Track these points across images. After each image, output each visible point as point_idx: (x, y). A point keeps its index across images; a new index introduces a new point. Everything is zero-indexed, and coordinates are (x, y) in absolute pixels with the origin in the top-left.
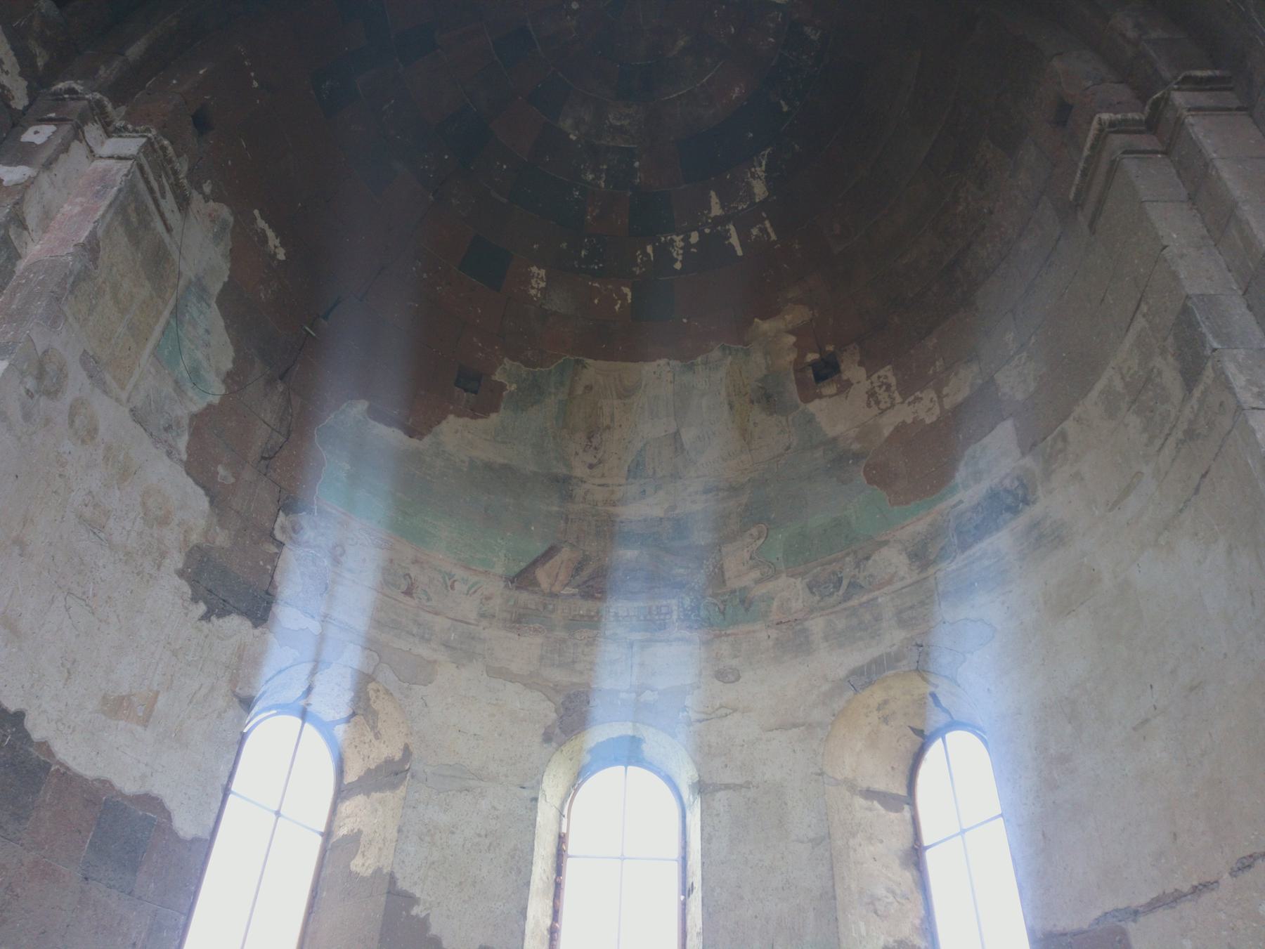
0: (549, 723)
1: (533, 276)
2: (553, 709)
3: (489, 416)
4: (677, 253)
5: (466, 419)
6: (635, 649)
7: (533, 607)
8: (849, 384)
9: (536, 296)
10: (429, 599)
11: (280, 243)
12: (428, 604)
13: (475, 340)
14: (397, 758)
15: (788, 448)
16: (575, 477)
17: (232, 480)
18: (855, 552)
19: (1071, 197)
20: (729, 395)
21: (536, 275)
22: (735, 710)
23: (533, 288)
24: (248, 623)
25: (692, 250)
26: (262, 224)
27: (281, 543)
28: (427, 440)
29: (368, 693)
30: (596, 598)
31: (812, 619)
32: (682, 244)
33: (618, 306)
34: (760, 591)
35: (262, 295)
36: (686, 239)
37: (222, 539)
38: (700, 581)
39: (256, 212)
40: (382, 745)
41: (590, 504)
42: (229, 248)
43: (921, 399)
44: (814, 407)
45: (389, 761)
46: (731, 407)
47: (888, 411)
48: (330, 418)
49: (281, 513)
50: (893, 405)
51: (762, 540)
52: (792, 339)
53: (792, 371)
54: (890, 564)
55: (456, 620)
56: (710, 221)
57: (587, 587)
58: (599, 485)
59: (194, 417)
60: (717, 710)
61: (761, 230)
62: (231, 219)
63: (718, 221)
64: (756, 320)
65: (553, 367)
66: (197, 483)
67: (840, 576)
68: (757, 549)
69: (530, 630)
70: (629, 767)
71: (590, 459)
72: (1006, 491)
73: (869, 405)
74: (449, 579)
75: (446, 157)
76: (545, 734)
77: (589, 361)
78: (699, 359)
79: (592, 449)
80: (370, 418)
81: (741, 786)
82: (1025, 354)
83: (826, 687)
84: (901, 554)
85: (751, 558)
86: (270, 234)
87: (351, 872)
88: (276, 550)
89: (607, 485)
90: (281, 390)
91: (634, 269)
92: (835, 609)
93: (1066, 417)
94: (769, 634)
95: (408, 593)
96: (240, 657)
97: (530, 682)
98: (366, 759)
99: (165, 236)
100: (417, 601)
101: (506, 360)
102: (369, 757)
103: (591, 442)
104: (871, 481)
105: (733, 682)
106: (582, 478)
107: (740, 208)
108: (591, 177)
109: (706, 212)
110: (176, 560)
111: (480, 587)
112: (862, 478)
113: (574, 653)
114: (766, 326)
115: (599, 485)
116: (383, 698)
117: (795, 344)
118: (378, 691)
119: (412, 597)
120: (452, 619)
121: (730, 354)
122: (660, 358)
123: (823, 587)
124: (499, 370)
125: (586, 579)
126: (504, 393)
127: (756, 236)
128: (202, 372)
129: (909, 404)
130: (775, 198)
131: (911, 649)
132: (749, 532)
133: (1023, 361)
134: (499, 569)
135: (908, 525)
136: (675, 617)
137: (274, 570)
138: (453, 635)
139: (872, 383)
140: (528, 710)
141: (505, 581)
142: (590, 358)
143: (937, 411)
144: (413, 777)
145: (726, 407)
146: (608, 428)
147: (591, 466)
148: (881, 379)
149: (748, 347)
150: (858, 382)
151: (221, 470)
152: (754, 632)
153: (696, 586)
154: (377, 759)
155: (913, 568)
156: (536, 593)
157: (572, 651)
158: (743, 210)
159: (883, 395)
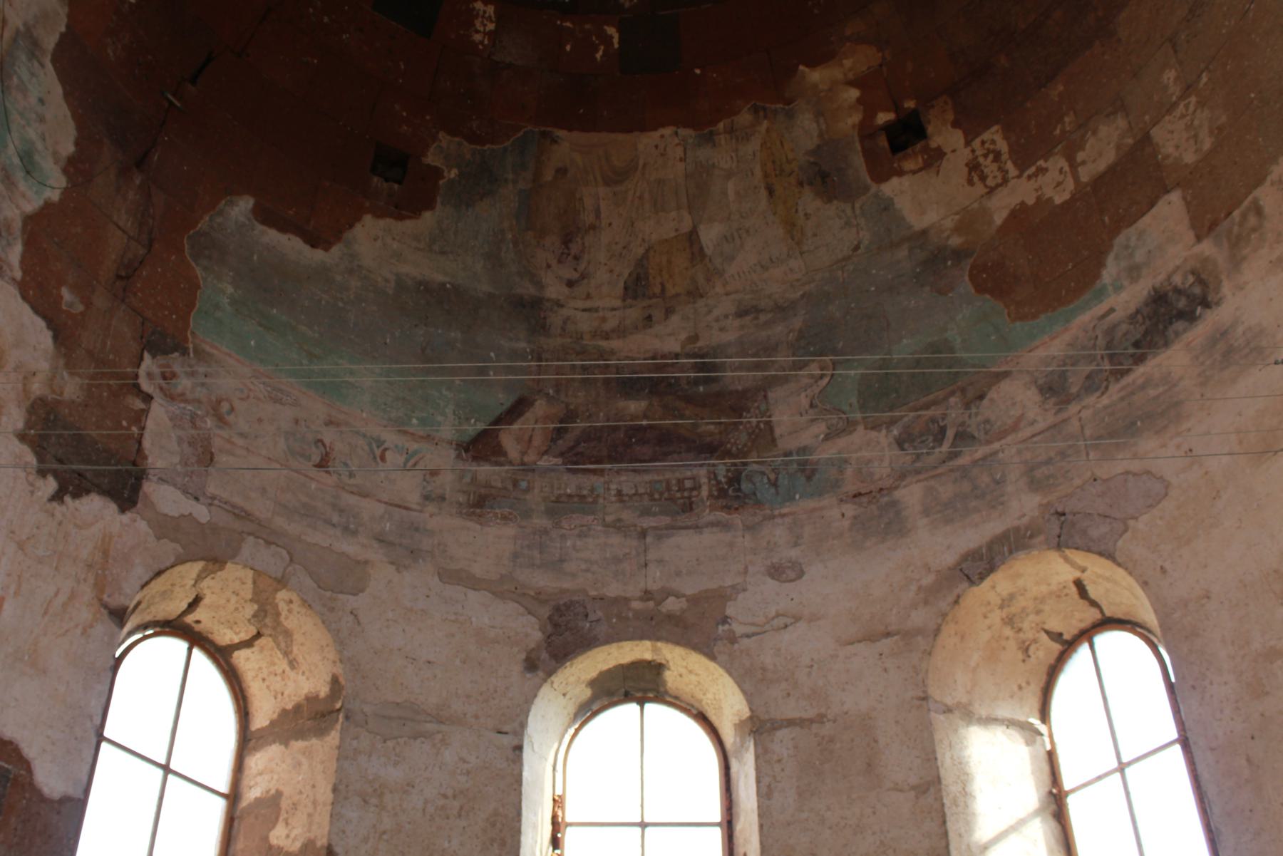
0: (532, 645)
1: (478, 14)
2: (537, 627)
3: (420, 214)
6: (649, 540)
7: (499, 485)
9: (482, 42)
10: (351, 475)
12: (352, 481)
13: (397, 107)
14: (322, 695)
15: (857, 248)
16: (548, 300)
17: (81, 308)
18: (963, 391)
20: (766, 176)
21: (481, 13)
22: (797, 619)
23: (477, 32)
24: (113, 507)
28: (336, 250)
29: (277, 606)
31: (905, 486)
34: (828, 452)
35: (110, 52)
37: (72, 388)
38: (738, 442)
41: (571, 337)
44: (891, 187)
45: (311, 699)
46: (771, 191)
48: (202, 221)
52: (854, 93)
53: (857, 139)
55: (391, 505)
58: (584, 310)
59: (29, 220)
60: (773, 619)
64: (801, 68)
65: (508, 144)
66: (36, 311)
67: (942, 424)
68: (821, 392)
69: (497, 517)
70: (648, 706)
71: (568, 273)
74: (378, 447)
77: (561, 133)
78: (721, 125)
79: (570, 258)
80: (257, 220)
81: (811, 721)
85: (812, 406)
87: (271, 847)
88: (142, 406)
92: (940, 471)
94: (844, 511)
95: (322, 464)
96: (106, 553)
97: (503, 589)
98: (279, 696)
100: (335, 477)
101: (441, 135)
102: (282, 694)
103: (568, 248)
106: (559, 300)
110: (16, 418)
111: (421, 459)
112: (966, 286)
113: (561, 548)
114: (816, 76)
115: (584, 310)
117: (859, 100)
118: (291, 602)
119: (328, 472)
120: (386, 503)
121: (765, 117)
123: (919, 441)
124: (432, 150)
125: (572, 444)
126: (441, 182)
128: (37, 158)
134: (447, 430)
136: (705, 492)
138: (388, 525)
140: (501, 628)
141: (456, 450)
142: (562, 128)
144: (347, 718)
145: (763, 193)
146: (593, 227)
147: (570, 284)
149: (791, 106)
151: (66, 294)
152: (822, 509)
153: (734, 449)
154: (295, 695)
157: (558, 545)
159: (990, 167)
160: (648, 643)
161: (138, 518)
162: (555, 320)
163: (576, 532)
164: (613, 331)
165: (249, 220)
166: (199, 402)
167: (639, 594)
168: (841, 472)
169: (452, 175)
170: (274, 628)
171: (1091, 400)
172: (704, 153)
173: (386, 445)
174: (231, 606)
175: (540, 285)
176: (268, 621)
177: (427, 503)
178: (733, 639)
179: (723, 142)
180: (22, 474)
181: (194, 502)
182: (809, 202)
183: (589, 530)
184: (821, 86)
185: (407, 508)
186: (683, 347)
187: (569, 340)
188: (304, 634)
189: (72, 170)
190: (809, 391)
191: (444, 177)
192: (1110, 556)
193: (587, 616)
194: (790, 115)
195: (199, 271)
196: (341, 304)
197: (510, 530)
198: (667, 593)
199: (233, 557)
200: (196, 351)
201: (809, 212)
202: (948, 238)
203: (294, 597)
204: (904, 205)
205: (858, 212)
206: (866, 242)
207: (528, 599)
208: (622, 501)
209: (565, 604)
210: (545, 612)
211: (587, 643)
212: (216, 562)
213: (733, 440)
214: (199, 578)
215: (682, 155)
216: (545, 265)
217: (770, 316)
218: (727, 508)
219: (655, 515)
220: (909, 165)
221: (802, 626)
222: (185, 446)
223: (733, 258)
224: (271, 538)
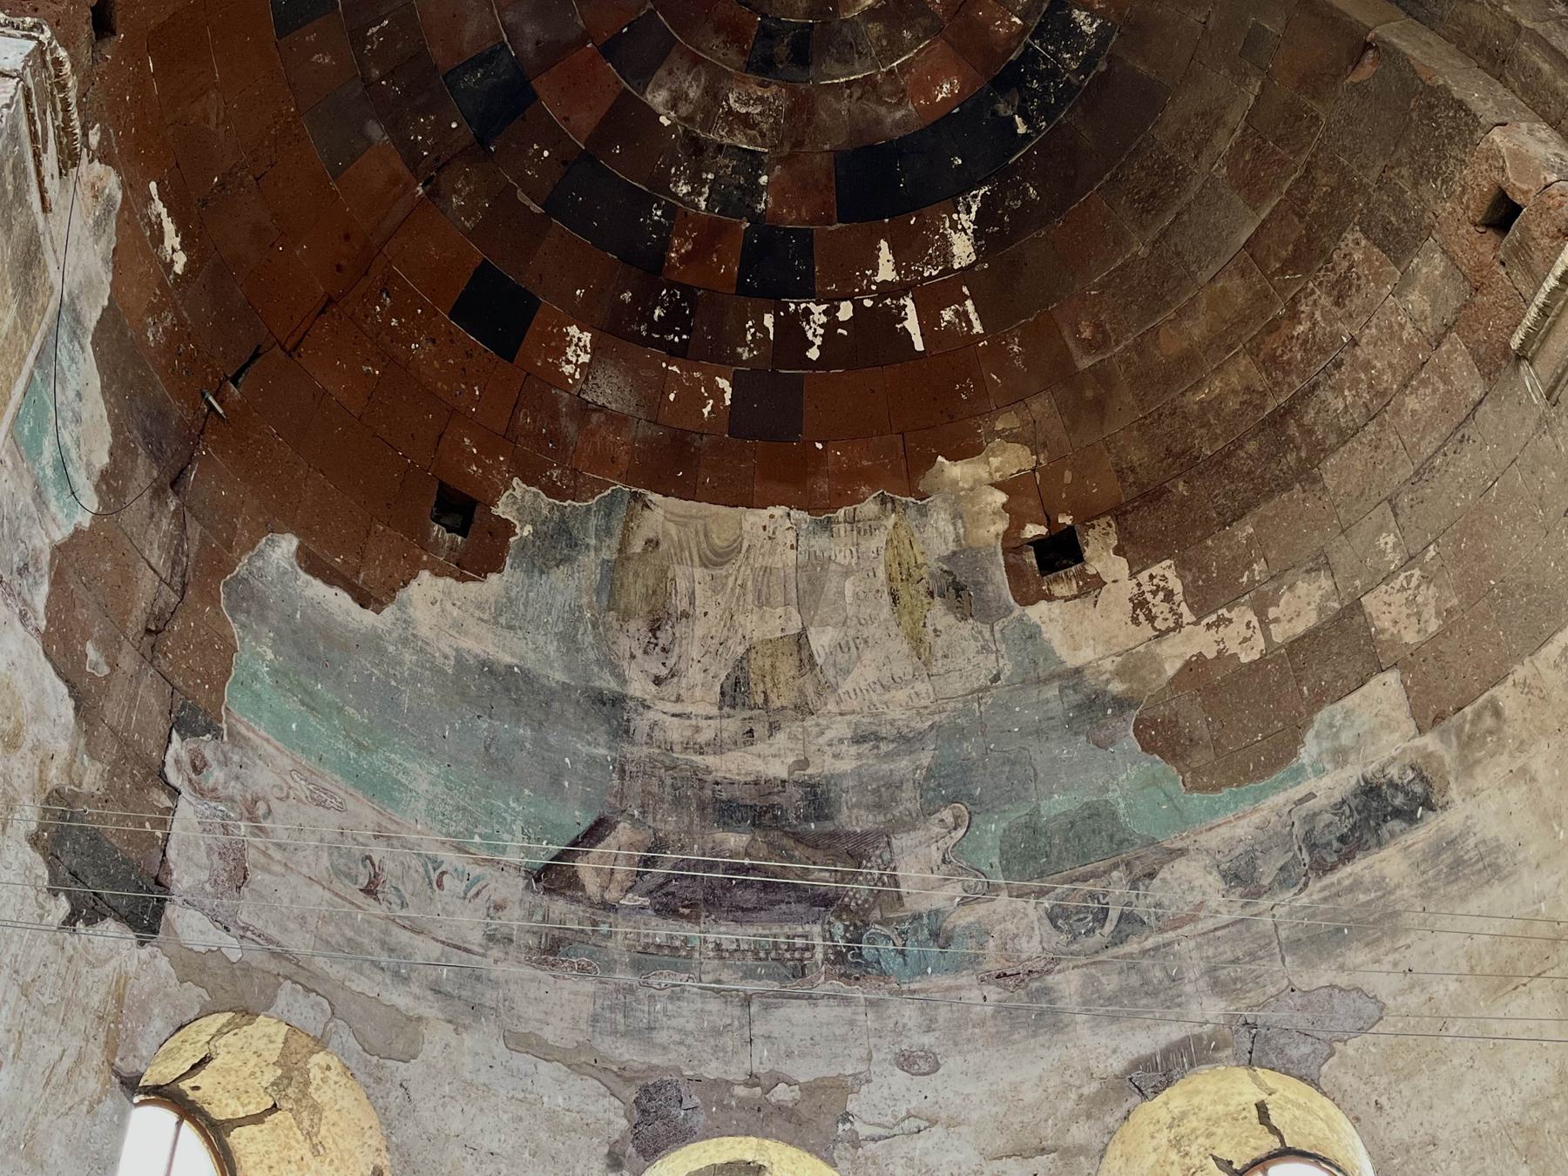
2: (622, 1112)
3: (485, 577)
4: (814, 332)
5: (449, 581)
6: (753, 1009)
8: (1098, 582)
9: (572, 376)
10: (403, 905)
11: (181, 244)
15: (996, 678)
17: (106, 670)
19: (1515, 343)
20: (890, 579)
21: (575, 340)
22: (933, 1122)
23: (569, 362)
25: (840, 331)
26: (159, 207)
27: (176, 790)
28: (389, 612)
30: (682, 916)
31: (1059, 971)
32: (824, 319)
33: (709, 408)
35: (150, 335)
36: (831, 312)
39: (153, 186)
40: (326, 1167)
41: (659, 747)
42: (112, 247)
43: (1230, 621)
46: (895, 599)
47: (1172, 634)
49: (175, 735)
50: (1178, 626)
51: (961, 832)
52: (1001, 498)
53: (1000, 551)
54: (1192, 889)
56: (874, 287)
57: (666, 895)
59: (59, 550)
61: (956, 312)
62: (119, 196)
63: (886, 289)
66: (59, 674)
69: (573, 968)
72: (1392, 784)
73: (1135, 620)
74: (435, 870)
75: (454, 125)
76: (610, 1154)
77: (655, 497)
78: (841, 512)
82: (1417, 572)
83: (1091, 1088)
84: (1210, 873)
85: (944, 861)
86: (169, 226)
89: (689, 718)
90: (172, 508)
91: (740, 350)
93: (1499, 680)
95: (370, 891)
96: (120, 1000)
99: (40, 217)
100: (385, 905)
101: (516, 481)
104: (1148, 747)
105: (924, 1074)
107: (926, 274)
108: (684, 189)
109: (869, 273)
110: (28, 816)
112: (1130, 742)
114: (956, 471)
115: (673, 715)
116: (336, 1083)
117: (1004, 506)
119: (377, 899)
120: (443, 943)
121: (893, 511)
122: (774, 505)
124: (503, 499)
125: (661, 880)
126: (512, 540)
127: (949, 322)
129: (1209, 626)
130: (986, 266)
131: (1237, 1031)
132: (937, 815)
133: (1414, 582)
135: (1219, 826)
136: (819, 956)
137: (167, 840)
139: (1139, 585)
143: (1259, 643)
145: (887, 599)
146: (685, 615)
147: (658, 681)
148: (1155, 581)
150: (1115, 581)
155: (1232, 898)
156: (579, 902)
158: (931, 277)
160: (753, 1140)
161: (159, 954)
162: (641, 724)
163: (668, 992)
164: (708, 745)
165: (292, 567)
166: (231, 799)
167: (742, 1077)
168: (981, 946)
169: (526, 533)
170: (297, 1101)
171: (1288, 895)
172: (820, 542)
173: (443, 868)
174: (246, 1071)
175: (624, 681)
176: (290, 1091)
177: (491, 944)
178: (856, 1143)
179: (842, 533)
180: (32, 893)
181: (224, 934)
182: (939, 615)
183: (683, 991)
184: (961, 484)
185: (467, 951)
186: (790, 773)
187: (657, 751)
188: (339, 1110)
189: (104, 487)
190: (940, 844)
191: (516, 534)
192: (1314, 1083)
193: (681, 1101)
194: (923, 512)
195: (235, 628)
196: (393, 683)
197: (588, 986)
198: (777, 1079)
199: (267, 1008)
200: (229, 735)
201: (939, 628)
202: (1108, 682)
203: (334, 1062)
204: (1053, 635)
205: (998, 636)
206: (1007, 672)
207: (614, 1075)
208: (722, 958)
209: (654, 1085)
210: (631, 1093)
211: (682, 1136)
212: (247, 1013)
213: (851, 894)
214: (220, 1033)
215: (794, 542)
216: (628, 655)
217: (892, 746)
218: (845, 976)
219: (760, 978)
220: (1060, 589)
221: (938, 1130)
222: (215, 857)
223: (849, 672)
224: (310, 984)
